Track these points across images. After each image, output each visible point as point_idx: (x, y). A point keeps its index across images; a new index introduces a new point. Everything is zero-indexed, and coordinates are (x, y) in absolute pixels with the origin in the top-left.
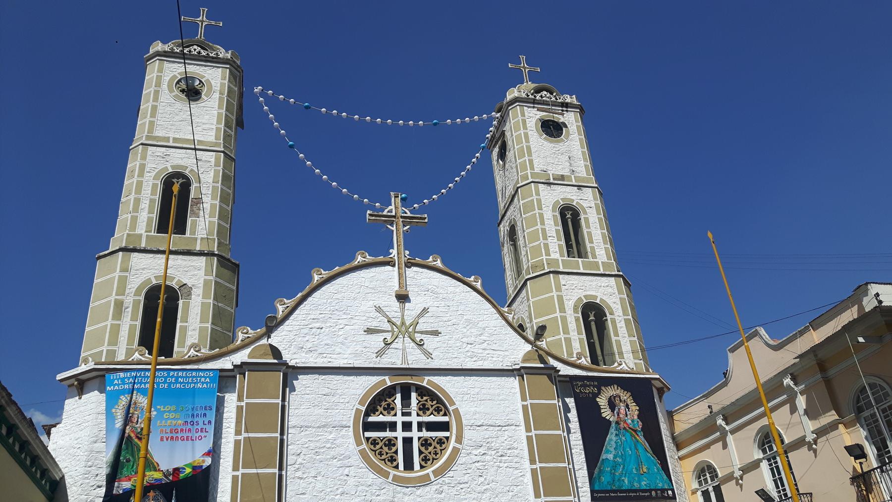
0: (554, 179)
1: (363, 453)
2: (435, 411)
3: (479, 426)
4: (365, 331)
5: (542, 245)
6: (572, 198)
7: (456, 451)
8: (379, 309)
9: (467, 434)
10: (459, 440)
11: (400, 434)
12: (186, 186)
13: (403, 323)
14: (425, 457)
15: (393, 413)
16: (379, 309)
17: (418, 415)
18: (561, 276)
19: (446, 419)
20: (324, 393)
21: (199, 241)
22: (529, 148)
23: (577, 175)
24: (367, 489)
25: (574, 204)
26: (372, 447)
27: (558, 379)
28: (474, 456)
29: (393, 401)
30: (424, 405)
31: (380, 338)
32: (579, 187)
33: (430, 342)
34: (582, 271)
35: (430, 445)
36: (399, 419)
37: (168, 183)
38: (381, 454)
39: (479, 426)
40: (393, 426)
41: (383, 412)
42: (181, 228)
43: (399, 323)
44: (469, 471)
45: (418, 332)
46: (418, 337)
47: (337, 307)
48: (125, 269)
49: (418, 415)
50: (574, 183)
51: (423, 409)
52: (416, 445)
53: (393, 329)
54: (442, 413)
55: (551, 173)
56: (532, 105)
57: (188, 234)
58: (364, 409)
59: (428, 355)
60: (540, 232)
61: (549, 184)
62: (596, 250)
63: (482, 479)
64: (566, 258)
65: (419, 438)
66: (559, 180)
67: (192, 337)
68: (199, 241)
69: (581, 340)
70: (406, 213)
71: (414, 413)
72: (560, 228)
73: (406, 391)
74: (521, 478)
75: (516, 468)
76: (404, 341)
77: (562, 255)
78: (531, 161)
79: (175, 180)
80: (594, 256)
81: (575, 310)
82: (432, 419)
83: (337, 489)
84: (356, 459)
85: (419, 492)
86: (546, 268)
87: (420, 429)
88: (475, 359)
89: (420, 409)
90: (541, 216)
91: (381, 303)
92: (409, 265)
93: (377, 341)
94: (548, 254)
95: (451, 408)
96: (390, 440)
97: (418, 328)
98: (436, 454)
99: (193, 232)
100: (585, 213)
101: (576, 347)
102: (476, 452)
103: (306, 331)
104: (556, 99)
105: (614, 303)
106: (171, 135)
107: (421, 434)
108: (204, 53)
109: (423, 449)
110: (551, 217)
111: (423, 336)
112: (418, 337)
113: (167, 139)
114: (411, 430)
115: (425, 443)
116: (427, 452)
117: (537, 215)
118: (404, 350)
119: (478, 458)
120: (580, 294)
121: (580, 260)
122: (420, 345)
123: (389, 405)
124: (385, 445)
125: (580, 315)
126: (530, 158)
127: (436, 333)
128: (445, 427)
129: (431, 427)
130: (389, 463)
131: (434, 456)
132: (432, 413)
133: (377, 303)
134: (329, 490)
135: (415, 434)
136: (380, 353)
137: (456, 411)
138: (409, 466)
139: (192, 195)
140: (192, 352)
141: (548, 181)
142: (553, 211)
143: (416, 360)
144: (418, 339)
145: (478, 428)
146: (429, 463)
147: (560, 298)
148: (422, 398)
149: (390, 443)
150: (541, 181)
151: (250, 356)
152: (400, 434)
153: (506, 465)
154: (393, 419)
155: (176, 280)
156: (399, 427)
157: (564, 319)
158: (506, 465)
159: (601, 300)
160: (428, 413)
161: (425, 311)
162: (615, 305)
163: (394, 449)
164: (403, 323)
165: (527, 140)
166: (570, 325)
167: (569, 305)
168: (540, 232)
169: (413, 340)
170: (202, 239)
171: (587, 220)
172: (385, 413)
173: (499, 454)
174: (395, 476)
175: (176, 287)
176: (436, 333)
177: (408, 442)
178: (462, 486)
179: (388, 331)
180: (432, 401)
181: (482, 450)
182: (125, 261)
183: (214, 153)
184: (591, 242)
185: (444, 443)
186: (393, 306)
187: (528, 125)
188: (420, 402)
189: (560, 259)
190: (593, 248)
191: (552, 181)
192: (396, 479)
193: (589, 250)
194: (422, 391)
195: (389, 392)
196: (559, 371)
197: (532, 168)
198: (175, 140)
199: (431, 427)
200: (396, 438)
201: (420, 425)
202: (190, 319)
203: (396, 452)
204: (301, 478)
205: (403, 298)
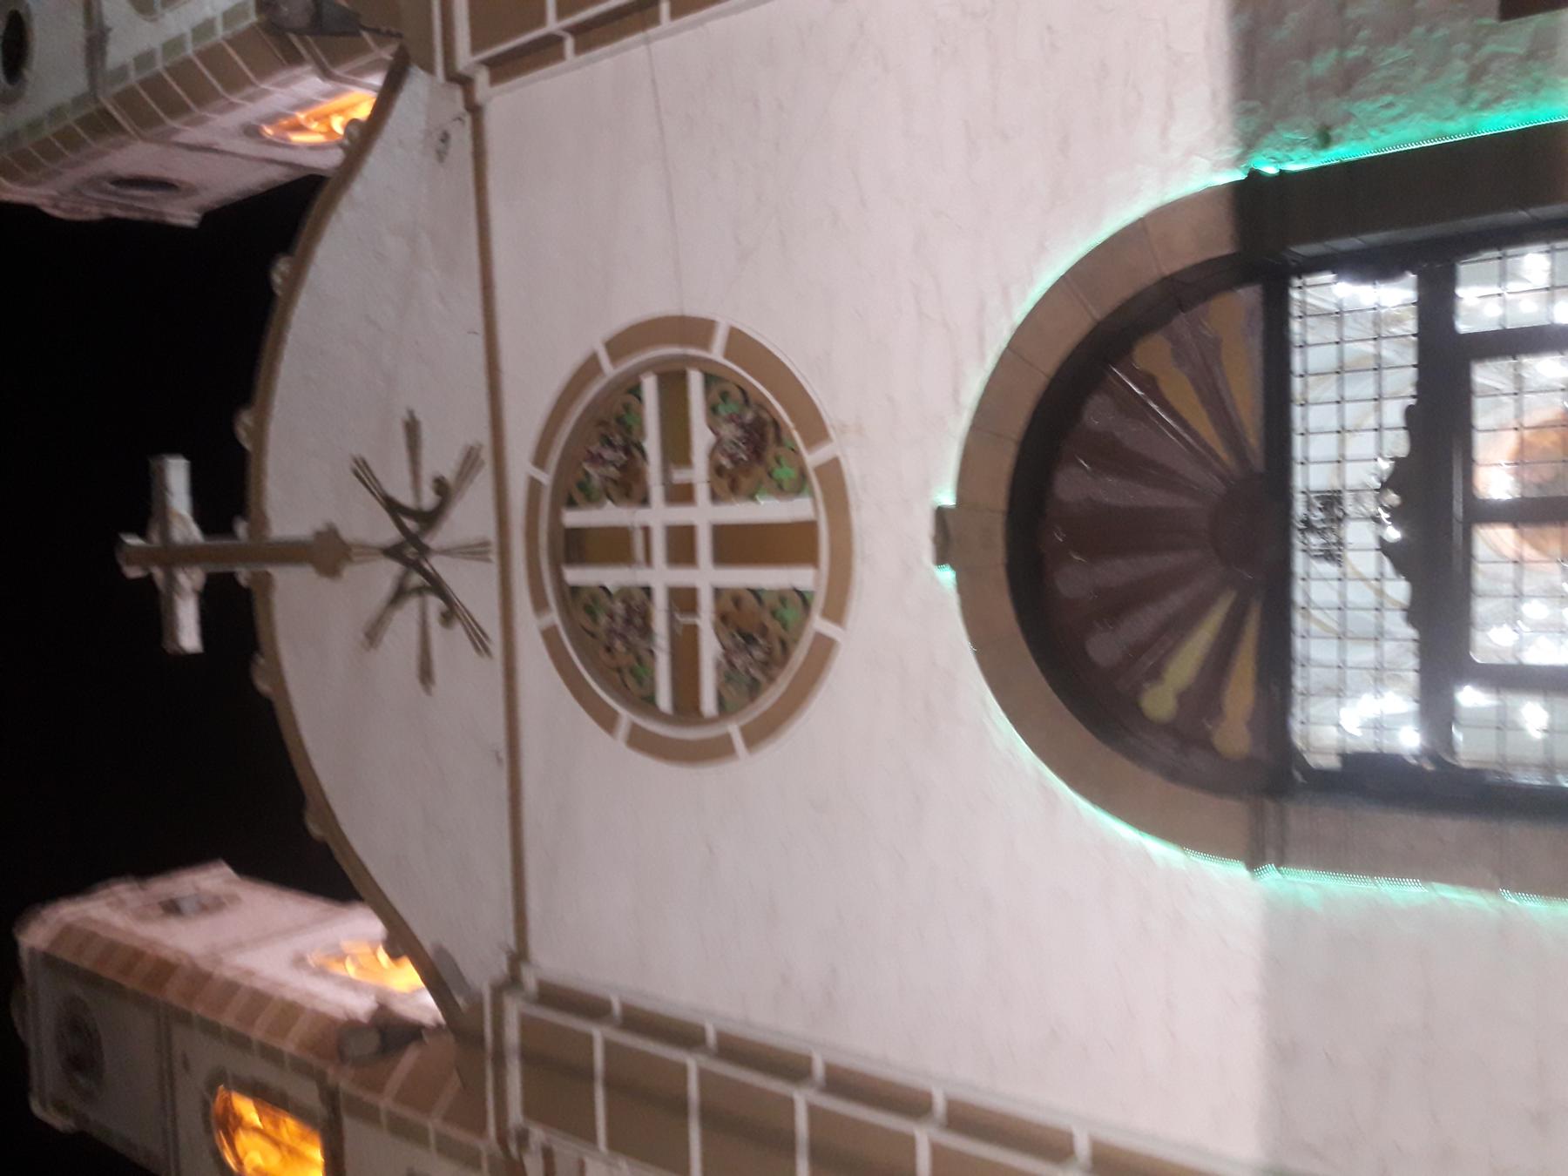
8: (373, 634)
52: (740, 512)
58: (626, 717)
93: (449, 645)
97: (405, 498)
107: (702, 492)
112: (429, 499)
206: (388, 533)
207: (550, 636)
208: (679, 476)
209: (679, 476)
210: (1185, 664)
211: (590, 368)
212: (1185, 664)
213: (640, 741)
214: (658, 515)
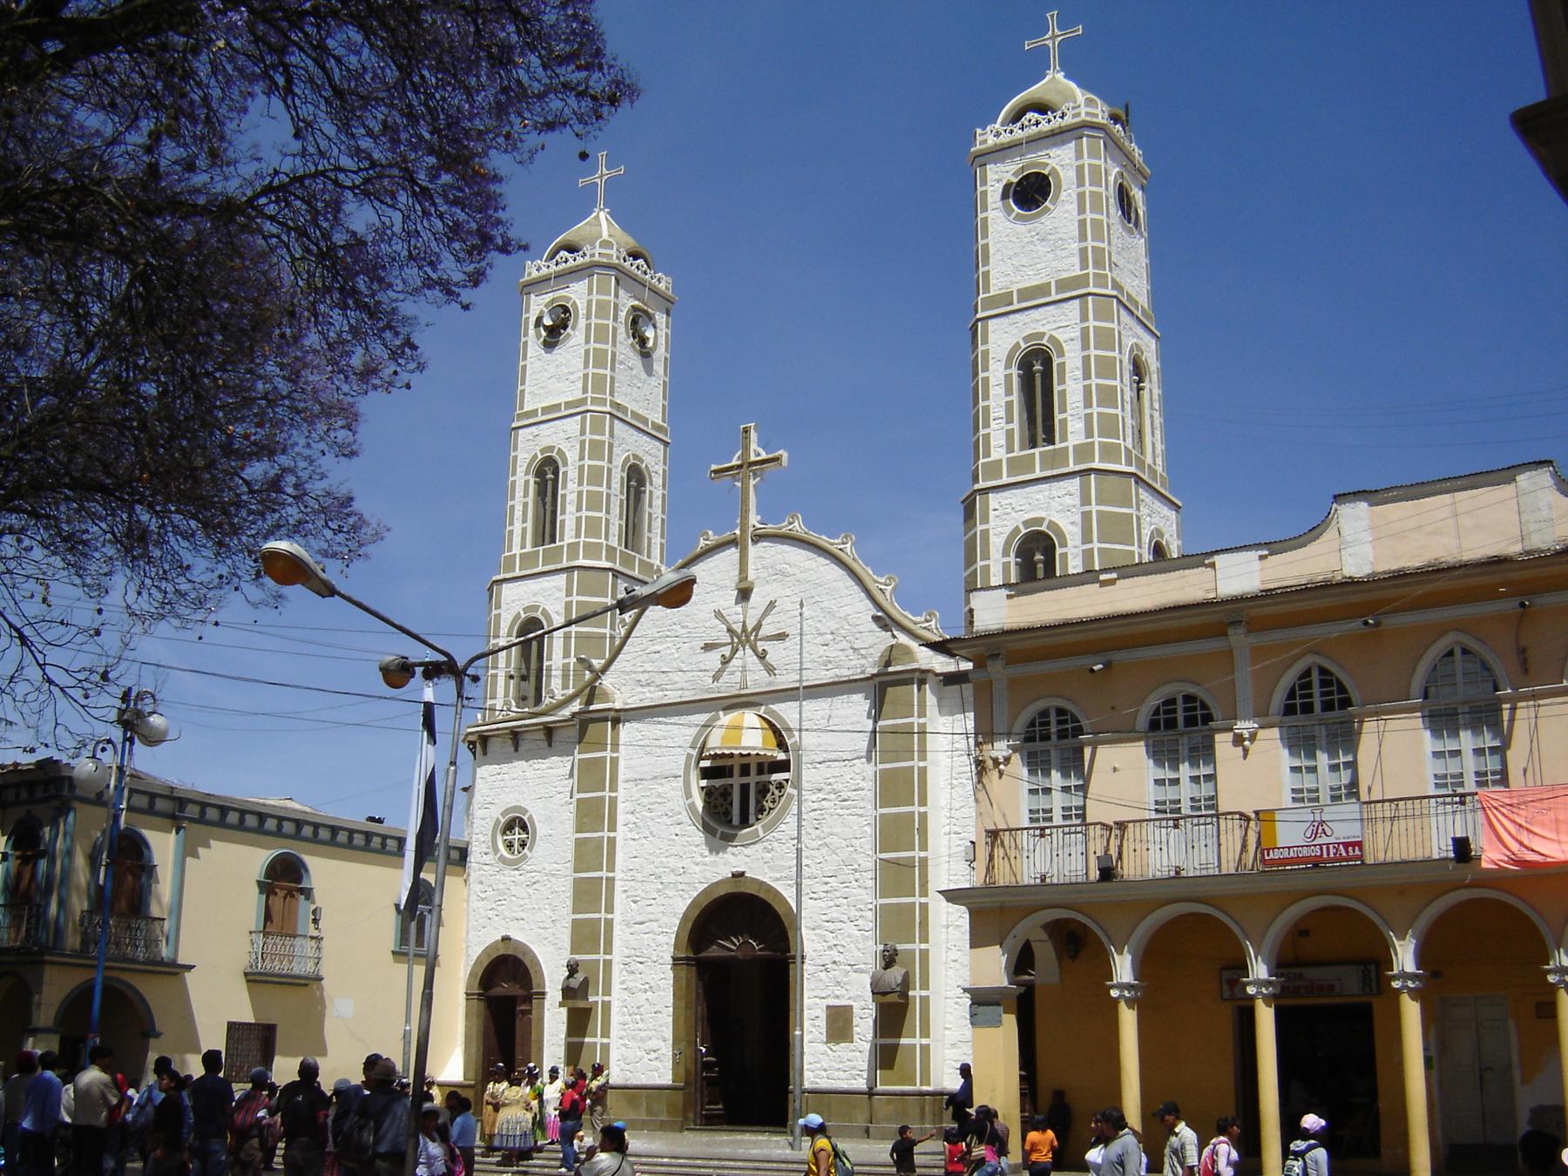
3: (820, 763)
6: (1042, 330)
8: (719, 615)
9: (809, 776)
16: (719, 615)
20: (655, 737)
24: (695, 849)
33: (775, 652)
34: (1038, 474)
38: (715, 807)
43: (739, 631)
45: (760, 640)
46: (761, 646)
47: (674, 620)
57: (558, 544)
59: (770, 670)
62: (1069, 424)
70: (759, 455)
75: (861, 816)
77: (1010, 449)
79: (547, 469)
81: (1006, 553)
83: (667, 851)
88: (830, 666)
92: (759, 538)
93: (714, 660)
97: (762, 633)
98: (773, 802)
100: (1061, 354)
103: (644, 658)
106: (540, 406)
112: (761, 646)
113: (534, 413)
114: (748, 775)
119: (815, 806)
122: (762, 656)
124: (721, 795)
130: (723, 817)
133: (715, 606)
134: (658, 852)
142: (1008, 366)
144: (760, 649)
145: (818, 766)
146: (765, 813)
155: (541, 609)
156: (736, 771)
161: (772, 605)
162: (1072, 528)
171: (1062, 366)
173: (840, 799)
177: (745, 789)
179: (729, 644)
181: (821, 796)
183: (579, 417)
198: (546, 410)
200: (732, 785)
203: (731, 804)
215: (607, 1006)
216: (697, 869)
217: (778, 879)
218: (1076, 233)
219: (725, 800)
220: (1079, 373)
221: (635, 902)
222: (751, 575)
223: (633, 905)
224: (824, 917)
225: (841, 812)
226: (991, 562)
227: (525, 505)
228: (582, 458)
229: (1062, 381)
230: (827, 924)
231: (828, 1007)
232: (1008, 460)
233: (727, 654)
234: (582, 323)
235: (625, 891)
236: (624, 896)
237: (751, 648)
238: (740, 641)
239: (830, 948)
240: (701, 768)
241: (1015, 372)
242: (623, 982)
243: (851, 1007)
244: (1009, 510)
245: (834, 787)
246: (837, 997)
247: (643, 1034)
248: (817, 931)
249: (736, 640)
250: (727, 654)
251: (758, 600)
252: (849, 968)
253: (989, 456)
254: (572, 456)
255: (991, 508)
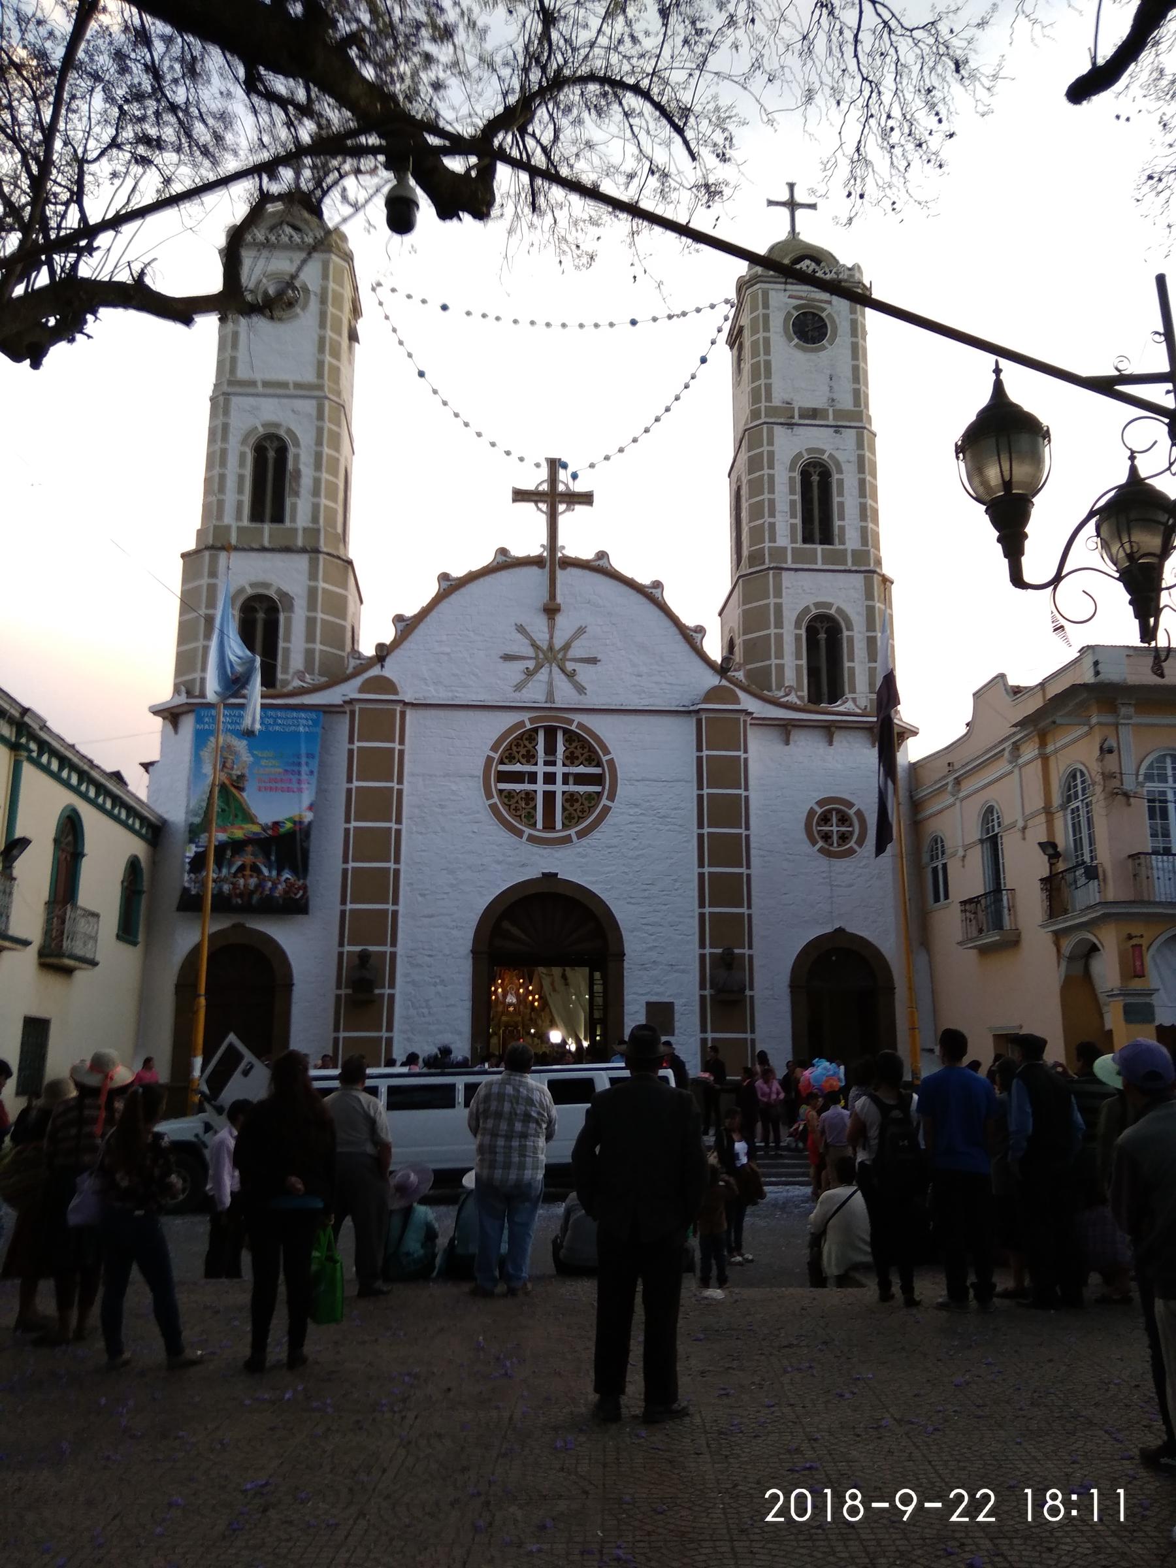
0: (801, 417)
1: (493, 807)
2: (586, 760)
3: (638, 781)
4: (501, 657)
5: (766, 525)
7: (607, 810)
8: (521, 629)
10: (611, 797)
11: (540, 787)
12: (282, 451)
13: (551, 648)
14: (570, 814)
15: (533, 761)
16: (521, 629)
17: (564, 765)
18: (785, 574)
19: (597, 770)
21: (300, 533)
22: (768, 364)
23: (839, 406)
24: (496, 848)
25: (825, 457)
26: (506, 800)
27: (748, 722)
28: (628, 817)
29: (534, 747)
30: (572, 753)
31: (520, 666)
32: (837, 429)
33: (585, 674)
35: (577, 800)
36: (541, 769)
37: (260, 451)
39: (638, 781)
40: (533, 778)
41: (522, 760)
42: (278, 517)
43: (545, 648)
44: (621, 834)
48: (213, 574)
49: (564, 765)
50: (831, 422)
51: (571, 759)
53: (537, 656)
54: (594, 763)
55: (796, 405)
56: (782, 286)
57: (288, 524)
59: (581, 689)
60: (766, 504)
61: (790, 425)
63: (635, 844)
64: (799, 545)
65: (564, 793)
66: (808, 418)
67: (297, 662)
68: (300, 533)
69: (798, 668)
71: (559, 763)
72: (797, 498)
73: (551, 733)
74: (686, 844)
76: (551, 671)
77: (793, 541)
78: (768, 388)
80: (842, 542)
81: (798, 625)
82: (581, 769)
83: (463, 847)
84: (486, 817)
85: (557, 855)
86: (767, 561)
87: (565, 782)
89: (567, 758)
90: (771, 478)
91: (523, 620)
94: (773, 539)
95: (604, 759)
96: (527, 793)
97: (572, 653)
99: (293, 520)
100: (840, 471)
101: (790, 678)
102: (632, 811)
104: (825, 273)
105: (858, 614)
107: (566, 788)
108: (297, 238)
109: (567, 805)
110: (785, 480)
111: (578, 666)
112: (570, 666)
113: (253, 383)
115: (570, 798)
116: (571, 809)
117: (766, 477)
118: (550, 684)
119: (633, 819)
120: (809, 600)
121: (819, 548)
122: (571, 675)
123: (528, 751)
125: (803, 632)
126: (769, 381)
127: (593, 661)
128: (597, 780)
129: (581, 779)
131: (580, 814)
132: (581, 763)
135: (559, 788)
136: (519, 687)
137: (611, 762)
138: (549, 825)
139: (290, 465)
140: (297, 683)
141: (789, 421)
142: (792, 469)
143: (565, 695)
145: (636, 783)
147: (779, 608)
148: (570, 744)
149: (530, 797)
150: (779, 421)
151: (361, 690)
152: (540, 787)
153: (667, 828)
154: (532, 769)
157: (779, 637)
158: (667, 828)
159: (839, 610)
160: (577, 762)
161: (581, 631)
163: (532, 805)
164: (551, 648)
165: (767, 352)
166: (785, 646)
167: (790, 617)
168: (766, 504)
169: (563, 670)
170: (305, 529)
171: (841, 482)
172: (523, 761)
174: (530, 836)
175: (275, 597)
176: (593, 661)
177: (549, 797)
178: (610, 850)
180: (583, 747)
182: (214, 562)
184: (842, 518)
185: (594, 799)
186: (538, 627)
187: (771, 323)
188: (567, 749)
189: (790, 546)
190: (842, 528)
191: (796, 420)
192: (532, 839)
193: (836, 531)
194: (570, 736)
195: (531, 735)
196: (752, 713)
197: (769, 398)
198: (266, 384)
199: (581, 779)
200: (535, 791)
201: (566, 777)
202: (293, 638)
203: (535, 808)
204: (421, 833)
205: (551, 611)
206: (558, 643)
207: (522, 724)
208: (571, 780)
209: (571, 780)
210: (515, 931)
211: (607, 752)
212: (515, 931)
213: (489, 760)
214: (559, 770)
215: (392, 998)
216: (499, 867)
217: (593, 883)
218: (850, 374)
219: (527, 804)
220: (856, 492)
221: (421, 895)
222: (559, 599)
223: (420, 899)
224: (644, 921)
225: (661, 827)
226: (784, 631)
227: (241, 478)
228: (319, 443)
229: (841, 494)
230: (644, 927)
231: (648, 1004)
232: (846, 550)
233: (531, 667)
234: (314, 305)
235: (411, 884)
236: (408, 888)
237: (559, 666)
238: (546, 658)
239: (651, 949)
240: (499, 772)
241: (797, 475)
242: (407, 975)
243: (672, 1003)
244: (800, 591)
245: (653, 803)
246: (657, 994)
247: (433, 1028)
248: (635, 933)
249: (541, 656)
250: (531, 667)
251: (565, 624)
252: (669, 968)
253: (775, 542)
254: (306, 438)
255: (784, 587)
